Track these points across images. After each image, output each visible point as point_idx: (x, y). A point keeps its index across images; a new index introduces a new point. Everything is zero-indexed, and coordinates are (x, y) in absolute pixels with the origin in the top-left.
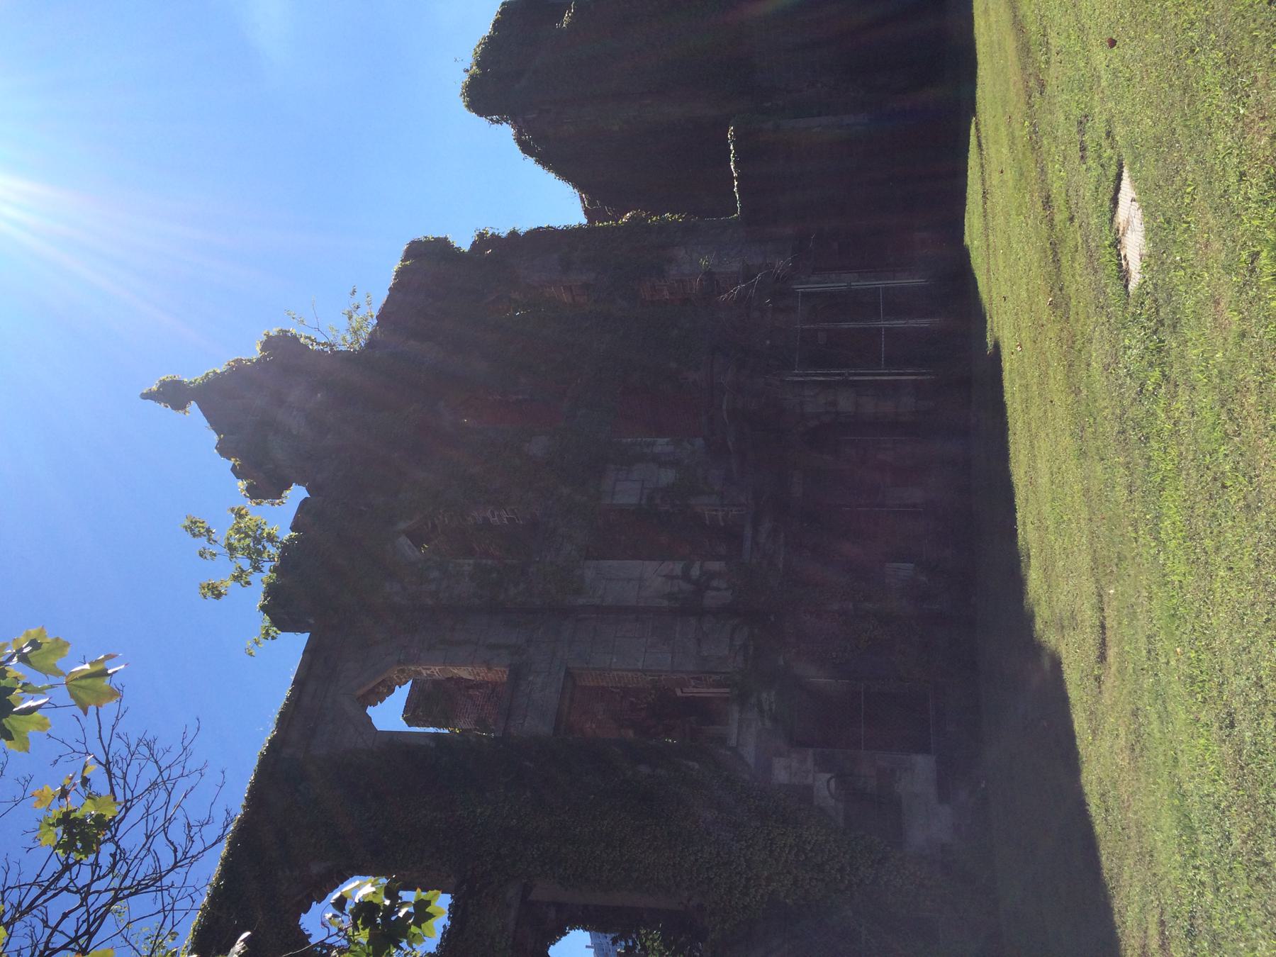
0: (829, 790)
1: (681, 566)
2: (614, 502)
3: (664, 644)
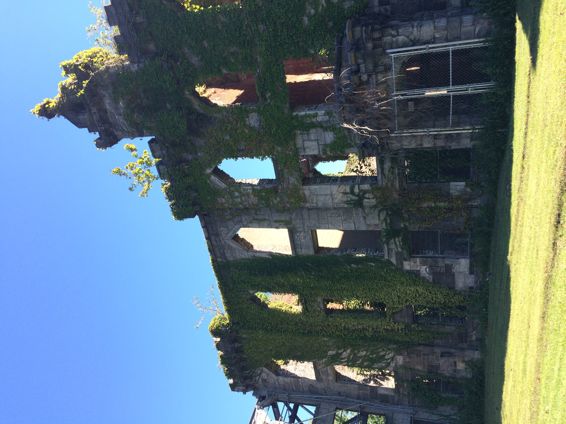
1: (349, 187)
2: (306, 154)
3: (349, 219)
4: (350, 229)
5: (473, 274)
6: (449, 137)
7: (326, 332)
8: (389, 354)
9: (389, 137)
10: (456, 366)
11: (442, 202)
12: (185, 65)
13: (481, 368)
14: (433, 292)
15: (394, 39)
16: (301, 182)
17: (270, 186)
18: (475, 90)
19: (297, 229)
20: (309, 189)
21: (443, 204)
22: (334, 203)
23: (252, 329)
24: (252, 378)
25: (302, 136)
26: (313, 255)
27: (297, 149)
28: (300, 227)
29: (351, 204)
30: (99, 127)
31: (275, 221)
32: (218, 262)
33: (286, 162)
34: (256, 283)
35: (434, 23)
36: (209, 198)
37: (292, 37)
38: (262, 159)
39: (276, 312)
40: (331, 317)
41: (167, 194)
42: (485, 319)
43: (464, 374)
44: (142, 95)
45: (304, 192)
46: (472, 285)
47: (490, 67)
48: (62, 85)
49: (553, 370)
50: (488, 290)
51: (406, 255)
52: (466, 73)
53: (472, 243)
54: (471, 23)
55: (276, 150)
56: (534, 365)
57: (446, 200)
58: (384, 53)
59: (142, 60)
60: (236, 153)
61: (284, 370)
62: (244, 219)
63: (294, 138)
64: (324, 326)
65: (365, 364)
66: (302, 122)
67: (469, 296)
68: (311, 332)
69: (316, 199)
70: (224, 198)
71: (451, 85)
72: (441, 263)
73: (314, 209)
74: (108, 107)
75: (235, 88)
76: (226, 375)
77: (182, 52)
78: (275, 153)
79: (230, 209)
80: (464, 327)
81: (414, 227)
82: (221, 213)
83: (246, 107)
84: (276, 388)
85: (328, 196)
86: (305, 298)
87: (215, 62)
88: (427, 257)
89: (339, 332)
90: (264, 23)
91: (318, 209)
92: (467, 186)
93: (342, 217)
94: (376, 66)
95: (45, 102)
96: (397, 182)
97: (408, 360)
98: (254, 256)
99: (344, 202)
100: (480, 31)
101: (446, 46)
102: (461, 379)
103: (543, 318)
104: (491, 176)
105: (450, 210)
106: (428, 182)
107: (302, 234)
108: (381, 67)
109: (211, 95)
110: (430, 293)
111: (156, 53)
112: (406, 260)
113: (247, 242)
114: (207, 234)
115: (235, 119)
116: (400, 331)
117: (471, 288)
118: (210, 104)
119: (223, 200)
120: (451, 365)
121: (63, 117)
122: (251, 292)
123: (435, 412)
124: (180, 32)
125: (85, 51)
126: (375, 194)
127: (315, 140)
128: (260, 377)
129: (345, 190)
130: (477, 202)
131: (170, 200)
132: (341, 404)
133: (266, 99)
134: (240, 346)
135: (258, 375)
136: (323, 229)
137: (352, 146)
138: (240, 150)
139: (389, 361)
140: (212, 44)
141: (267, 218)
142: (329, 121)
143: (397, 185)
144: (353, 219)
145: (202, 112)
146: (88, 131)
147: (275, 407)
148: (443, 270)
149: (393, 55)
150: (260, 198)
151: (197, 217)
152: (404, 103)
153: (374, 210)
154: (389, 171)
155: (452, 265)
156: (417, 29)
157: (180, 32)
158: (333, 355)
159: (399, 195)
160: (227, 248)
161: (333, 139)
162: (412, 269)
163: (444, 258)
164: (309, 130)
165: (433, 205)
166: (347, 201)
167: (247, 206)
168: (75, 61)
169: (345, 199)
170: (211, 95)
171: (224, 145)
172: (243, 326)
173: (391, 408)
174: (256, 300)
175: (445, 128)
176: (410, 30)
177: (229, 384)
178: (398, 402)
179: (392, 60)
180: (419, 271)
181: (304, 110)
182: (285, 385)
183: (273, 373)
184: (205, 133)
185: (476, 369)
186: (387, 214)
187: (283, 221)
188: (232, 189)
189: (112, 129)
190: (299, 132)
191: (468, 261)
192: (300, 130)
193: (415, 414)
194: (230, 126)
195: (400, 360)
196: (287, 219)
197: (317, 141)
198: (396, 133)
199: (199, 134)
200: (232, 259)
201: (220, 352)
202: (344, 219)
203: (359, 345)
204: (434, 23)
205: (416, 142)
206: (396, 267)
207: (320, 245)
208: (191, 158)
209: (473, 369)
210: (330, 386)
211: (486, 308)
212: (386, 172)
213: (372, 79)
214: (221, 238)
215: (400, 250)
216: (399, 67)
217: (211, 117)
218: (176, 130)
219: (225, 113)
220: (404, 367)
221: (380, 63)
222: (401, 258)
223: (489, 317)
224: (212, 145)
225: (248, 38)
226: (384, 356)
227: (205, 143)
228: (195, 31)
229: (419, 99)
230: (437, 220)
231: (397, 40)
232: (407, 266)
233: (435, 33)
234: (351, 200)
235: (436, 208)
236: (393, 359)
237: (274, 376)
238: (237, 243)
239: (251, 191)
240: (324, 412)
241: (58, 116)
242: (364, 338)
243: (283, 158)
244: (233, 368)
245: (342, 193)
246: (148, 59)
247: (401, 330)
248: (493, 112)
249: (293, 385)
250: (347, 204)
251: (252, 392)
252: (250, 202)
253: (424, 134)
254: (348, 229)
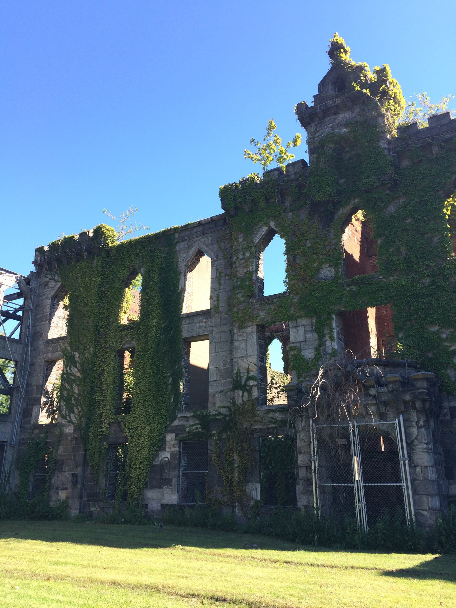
0: (164, 458)
2: (290, 329)
3: (220, 375)
4: (209, 376)
5: (161, 508)
6: (309, 482)
7: (99, 350)
8: (76, 418)
9: (309, 418)
10: (62, 490)
11: (239, 474)
12: (386, 198)
13: (61, 517)
14: (142, 465)
15: (414, 424)
16: (260, 323)
17: (256, 290)
18: (360, 510)
19: (209, 319)
20: (252, 332)
21: (236, 475)
23: (102, 271)
24: (49, 270)
25: (309, 325)
26: (182, 336)
27: (296, 319)
28: (212, 322)
29: (237, 377)
30: (320, 107)
31: (218, 296)
32: (174, 234)
33: (282, 307)
34: (151, 275)
35: (432, 466)
36: (243, 224)
37: (416, 314)
38: (285, 282)
39: (120, 297)
40: (115, 356)
41: (248, 179)
42: (113, 521)
43: (54, 498)
44: (353, 153)
45: (249, 326)
46: (150, 507)
47: (384, 526)
48: (365, 66)
49: (58, 594)
50: (144, 524)
51: (181, 436)
52: (378, 500)
53: (195, 506)
54: (431, 505)
55: (295, 297)
56: (63, 574)
57: (241, 479)
58: (399, 413)
59: (391, 152)
60: (291, 253)
61: (58, 305)
62: (220, 262)
63: (308, 315)
64: (106, 348)
65: (65, 393)
66: (324, 324)
67: (138, 504)
68: (99, 334)
69: (241, 340)
70: (243, 240)
71: (364, 484)
72: (173, 474)
73: (232, 337)
74: (341, 116)
75: (361, 252)
76: (53, 243)
77: (400, 196)
78: (291, 295)
79: (231, 247)
80: (104, 499)
81: (212, 445)
82: (227, 238)
83: (341, 264)
84: (39, 296)
85: (245, 353)
86: (135, 327)
87: (390, 232)
88: (179, 458)
89: (99, 364)
90: (432, 283)
91: (232, 342)
92: (256, 501)
93: (222, 368)
94: (385, 403)
95: (346, 48)
96: (260, 427)
97: (69, 438)
98: (180, 273)
99: (238, 370)
100: (423, 515)
101: (406, 479)
102: (48, 495)
103: (114, 583)
104: (267, 527)
105: (231, 483)
106: (260, 460)
107: (205, 325)
108: (384, 410)
109: (354, 227)
110: (141, 462)
111: (399, 167)
112: (176, 436)
113: (196, 266)
114: (205, 223)
115: (328, 252)
116: (100, 430)
117: (146, 506)
118: (344, 226)
119: (240, 240)
120: (63, 485)
121: (330, 68)
122: (142, 270)
123: (13, 467)
124: (421, 193)
125: (401, 91)
126: (247, 403)
127: (305, 338)
128: (50, 279)
129: (252, 371)
130: (239, 513)
131: (241, 183)
132: (22, 366)
133: (349, 285)
134: (84, 258)
135: (52, 277)
136: (210, 347)
137: (299, 378)
138: (294, 257)
139: (68, 418)
140: (409, 228)
141: (222, 287)
143: (257, 427)
144: (221, 379)
145: (336, 217)
146: (315, 94)
147: (18, 296)
148: (166, 476)
149: (397, 422)
150: (243, 280)
151: (223, 211)
152: (345, 433)
153: (230, 402)
154: (272, 418)
155: (171, 485)
156: (425, 448)
157: (421, 193)
158: (74, 358)
159: (246, 429)
160: (190, 243)
161: (306, 357)
162: (167, 443)
163: (179, 477)
164: (317, 332)
165: (236, 465)
166: (240, 373)
167: (234, 266)
168: (391, 80)
169: (242, 371)
170: (354, 227)
171: (300, 241)
172: (105, 261)
173: (17, 419)
174: (133, 275)
175: (319, 478)
176: (423, 441)
177: (43, 246)
178: (24, 427)
179: (392, 421)
180: (165, 450)
181: (338, 326)
182: (42, 306)
183: (55, 293)
184: (313, 221)
185: (59, 511)
186: (226, 416)
187: (218, 304)
188: (253, 249)
189: (318, 120)
190: (314, 321)
191: (176, 503)
192: (317, 322)
193: (10, 446)
194: (321, 247)
195: (69, 430)
196: (220, 308)
197: (304, 340)
198: (312, 425)
199: (312, 214)
200: (178, 249)
201: (78, 236)
202: (221, 370)
203: (85, 386)
204: (432, 466)
205: (303, 446)
206: (168, 426)
207: (193, 344)
208: (286, 205)
209: (59, 508)
210: (41, 354)
211: (126, 522)
212: (271, 415)
213: (371, 400)
214: (200, 238)
215: (187, 429)
216: (384, 428)
217: (330, 226)
218: (317, 189)
219: (334, 241)
220: (62, 434)
221: (388, 408)
222: (178, 431)
223: (116, 525)
224: (300, 228)
225: (415, 266)
226: (73, 413)
227: (303, 220)
228: (423, 210)
229: (349, 451)
230: (220, 469)
231: (413, 426)
232: (170, 437)
233: (420, 467)
234: (241, 378)
235: (233, 468)
236: (70, 422)
237: (52, 294)
238: (195, 255)
239: (251, 270)
240: (13, 348)
241: (331, 63)
242: (92, 391)
243: (286, 304)
244: (60, 250)
245: (249, 367)
246: (392, 159)
247: (102, 431)
248: (335, 530)
249: (42, 315)
250: (237, 373)
251: (35, 271)
252: (239, 269)
253: (312, 455)
254: (209, 373)
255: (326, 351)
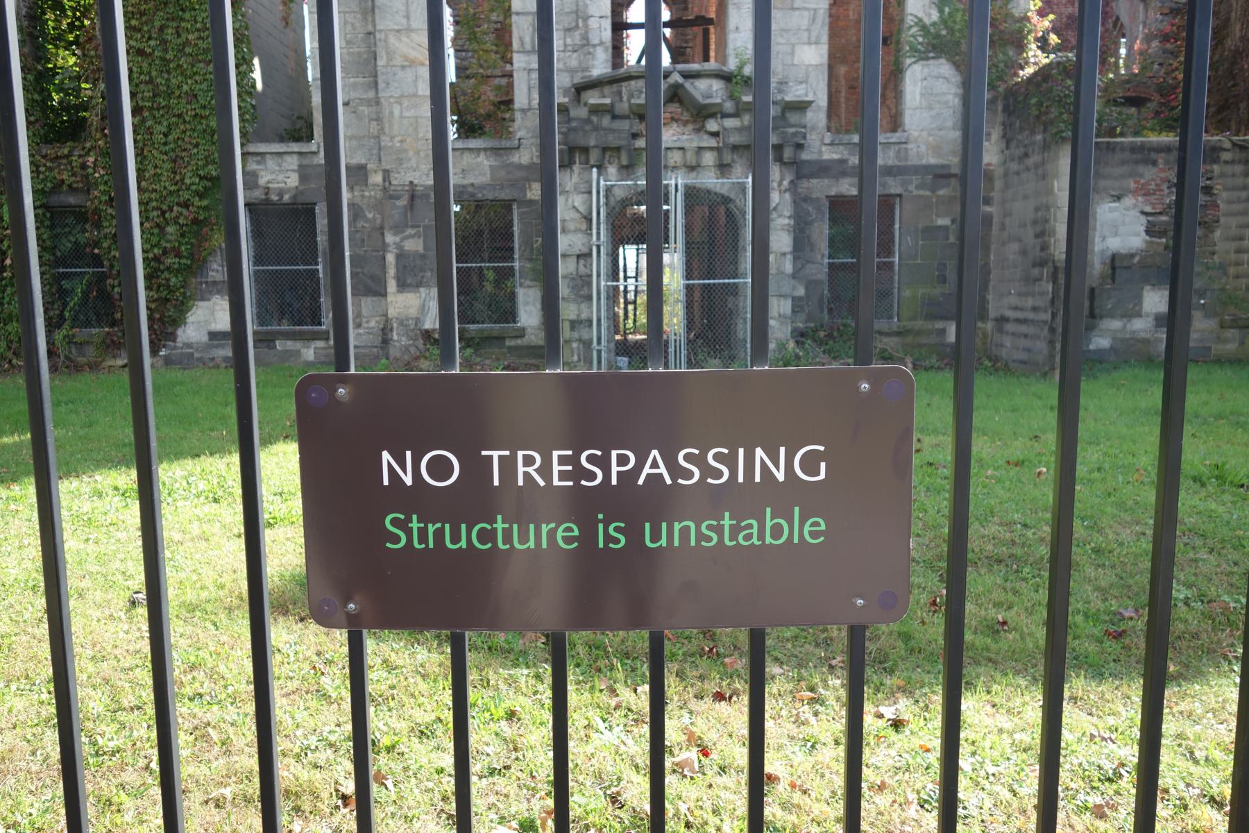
5: (210, 340)
22: (386, 36)
85: (404, 21)
142: (588, 44)
205: (574, 220)
255: (587, 39)
